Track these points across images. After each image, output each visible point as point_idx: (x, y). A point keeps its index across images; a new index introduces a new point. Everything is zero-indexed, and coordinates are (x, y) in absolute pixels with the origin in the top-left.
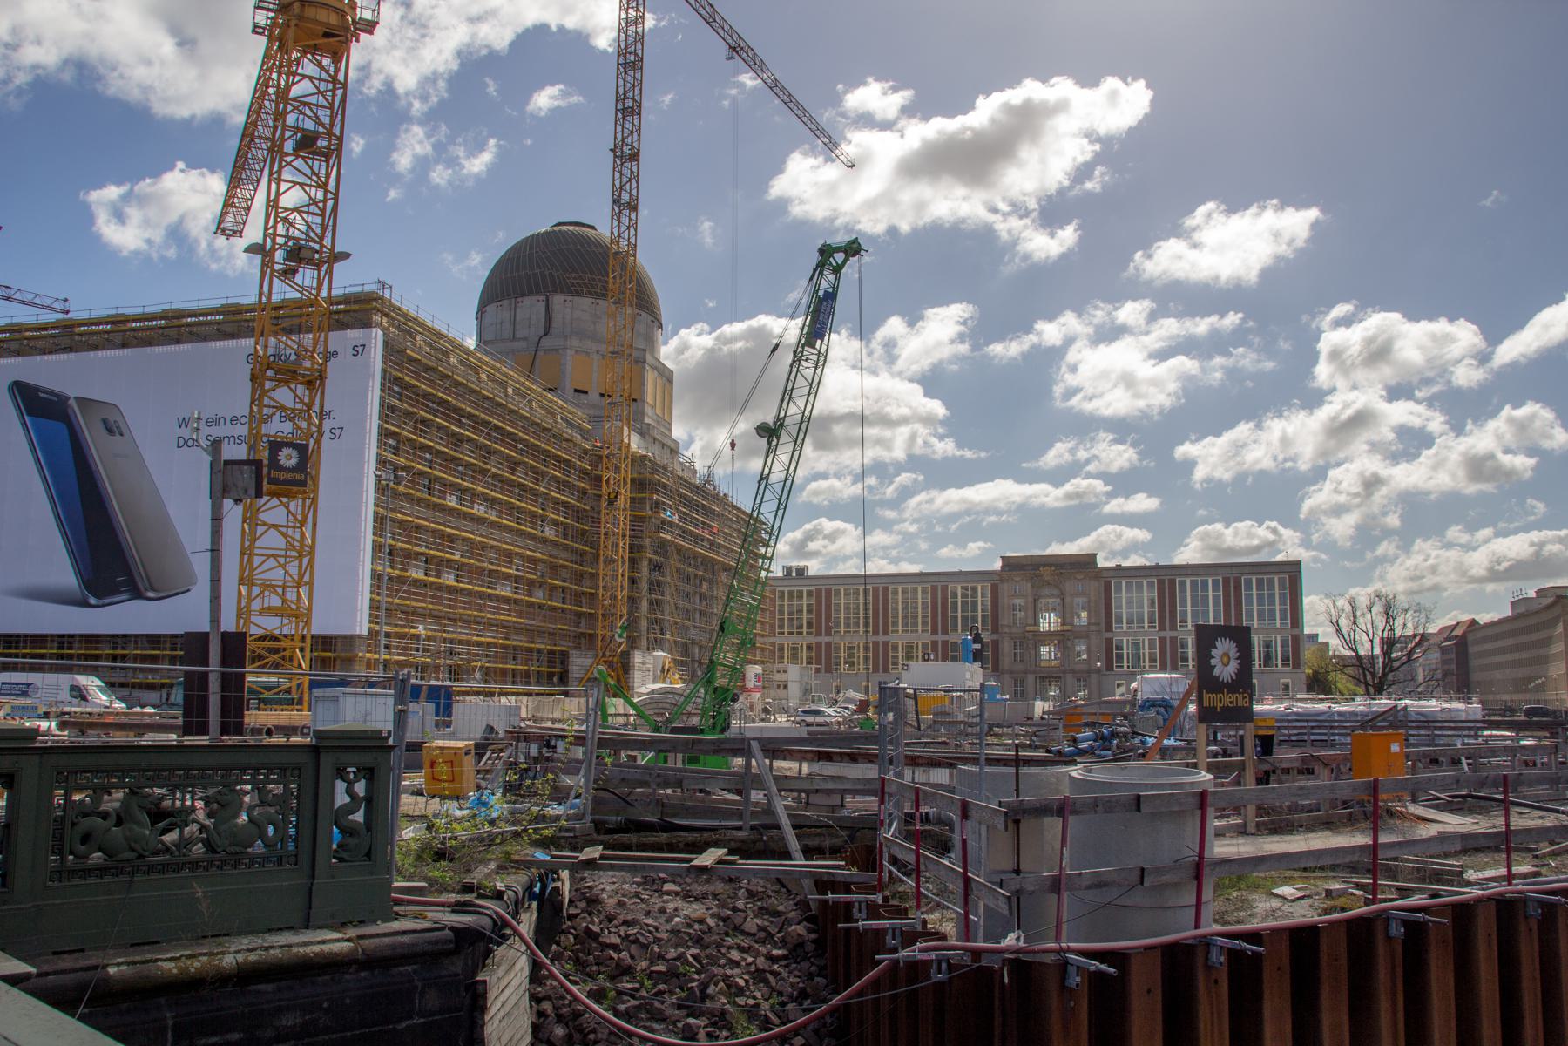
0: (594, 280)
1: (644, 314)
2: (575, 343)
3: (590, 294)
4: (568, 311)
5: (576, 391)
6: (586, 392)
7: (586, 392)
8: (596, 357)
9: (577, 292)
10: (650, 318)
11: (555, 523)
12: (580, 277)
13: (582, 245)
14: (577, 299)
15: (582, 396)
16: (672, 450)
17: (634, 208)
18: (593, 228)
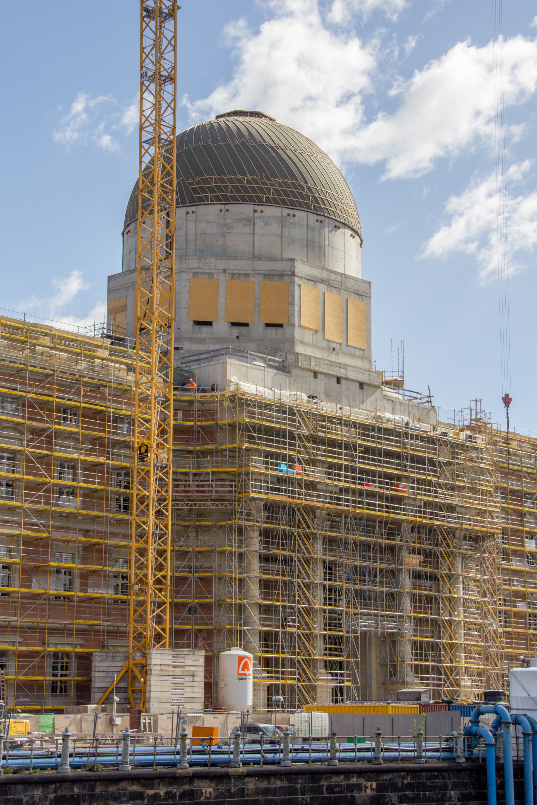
0: (222, 181)
1: (301, 215)
2: (194, 263)
3: (217, 199)
4: (191, 225)
5: (198, 323)
6: (210, 324)
7: (210, 324)
8: (222, 278)
9: (201, 199)
10: (312, 218)
11: (73, 492)
12: (206, 181)
13: (215, 140)
14: (201, 209)
15: (205, 329)
16: (361, 385)
17: (172, 79)
18: (259, 115)
